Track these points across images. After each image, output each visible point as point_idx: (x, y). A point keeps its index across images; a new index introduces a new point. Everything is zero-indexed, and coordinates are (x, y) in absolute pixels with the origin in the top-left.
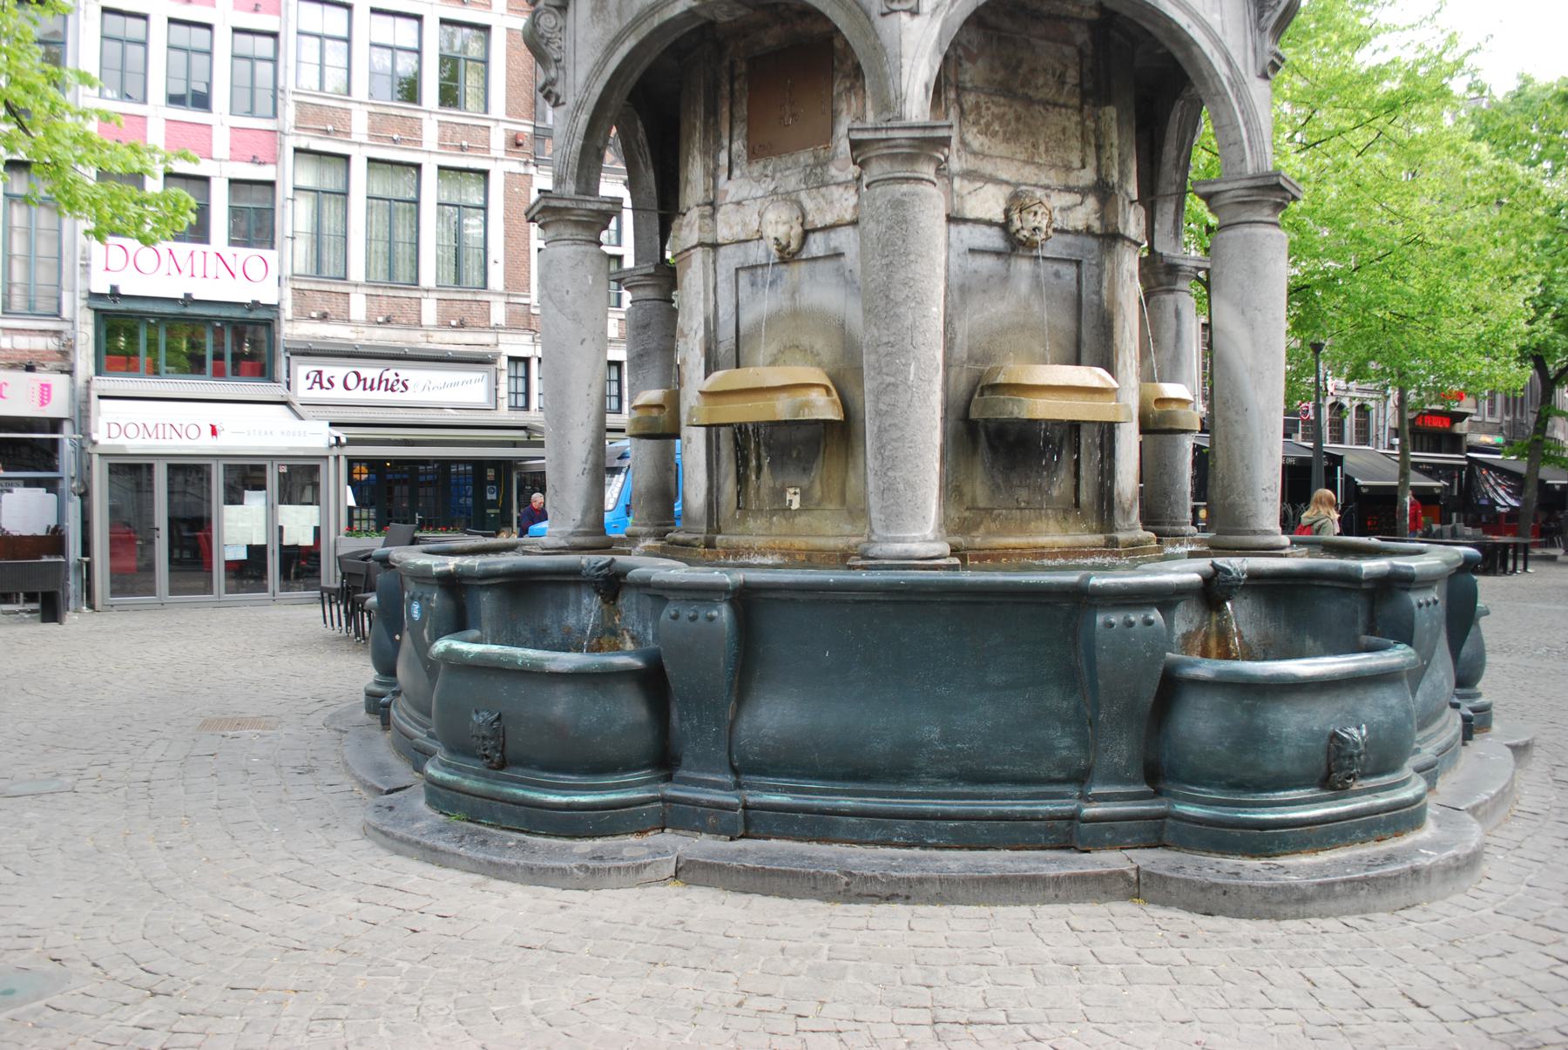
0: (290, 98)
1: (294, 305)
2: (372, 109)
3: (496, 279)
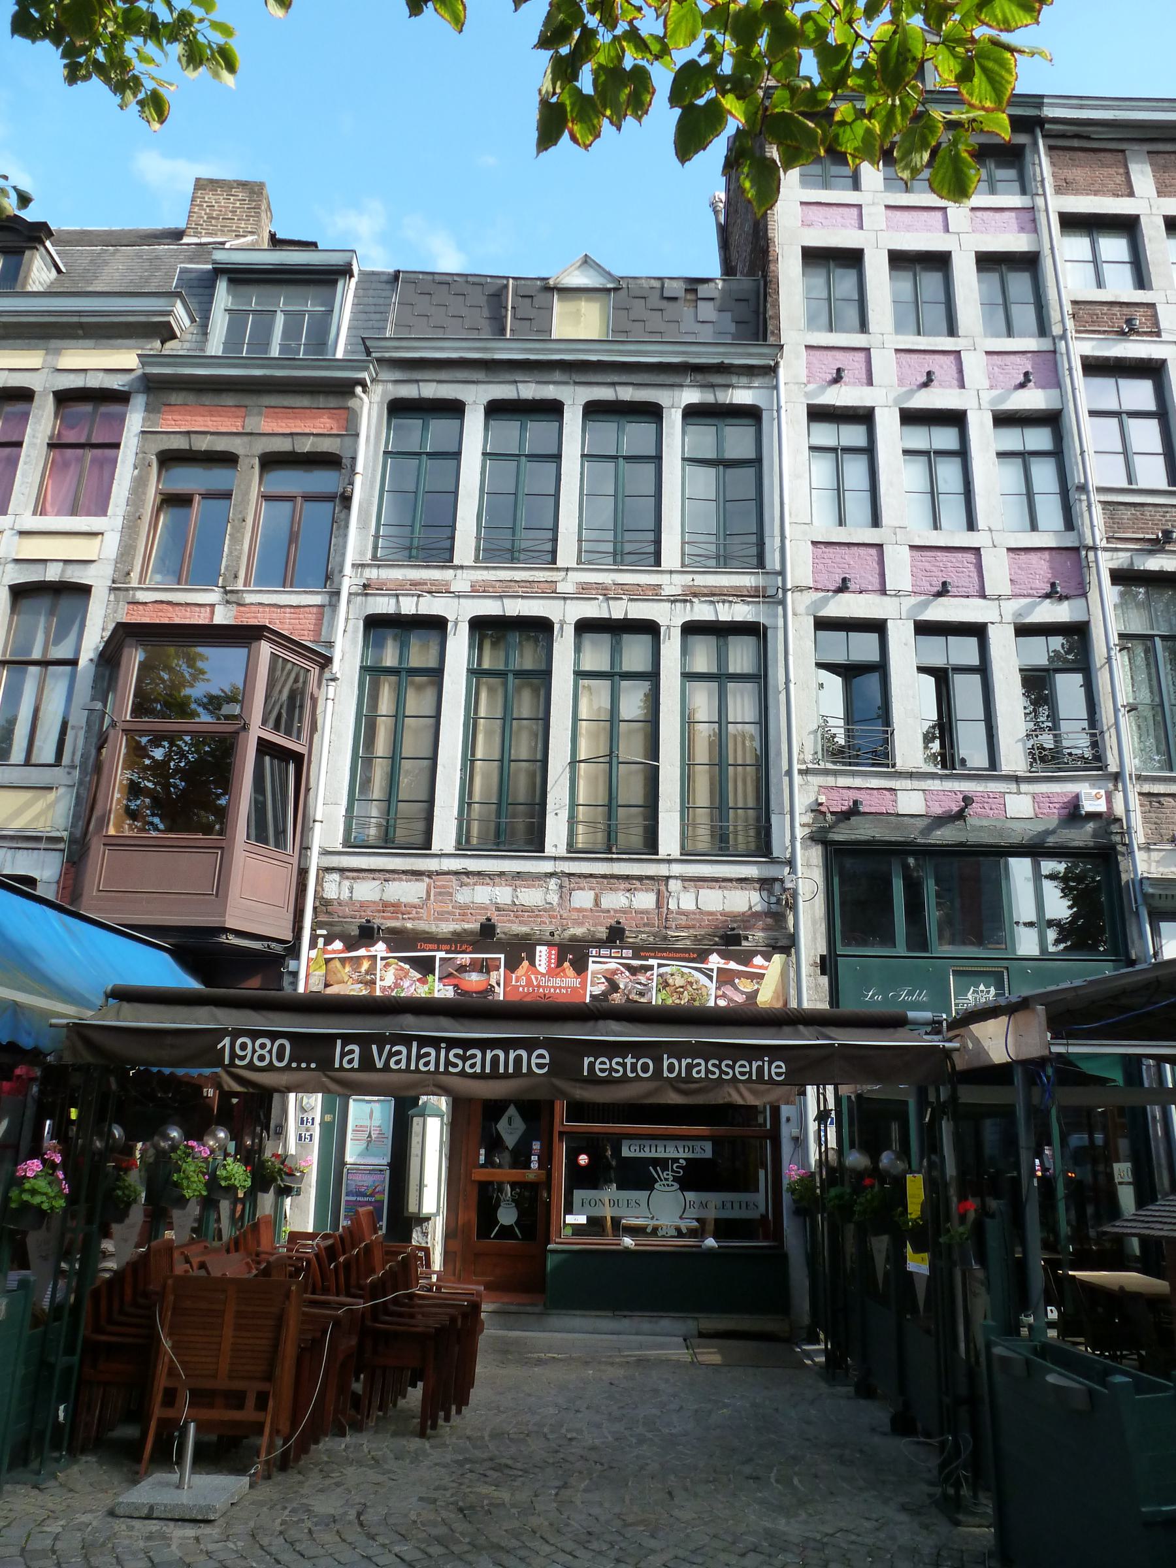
0: (1095, 497)
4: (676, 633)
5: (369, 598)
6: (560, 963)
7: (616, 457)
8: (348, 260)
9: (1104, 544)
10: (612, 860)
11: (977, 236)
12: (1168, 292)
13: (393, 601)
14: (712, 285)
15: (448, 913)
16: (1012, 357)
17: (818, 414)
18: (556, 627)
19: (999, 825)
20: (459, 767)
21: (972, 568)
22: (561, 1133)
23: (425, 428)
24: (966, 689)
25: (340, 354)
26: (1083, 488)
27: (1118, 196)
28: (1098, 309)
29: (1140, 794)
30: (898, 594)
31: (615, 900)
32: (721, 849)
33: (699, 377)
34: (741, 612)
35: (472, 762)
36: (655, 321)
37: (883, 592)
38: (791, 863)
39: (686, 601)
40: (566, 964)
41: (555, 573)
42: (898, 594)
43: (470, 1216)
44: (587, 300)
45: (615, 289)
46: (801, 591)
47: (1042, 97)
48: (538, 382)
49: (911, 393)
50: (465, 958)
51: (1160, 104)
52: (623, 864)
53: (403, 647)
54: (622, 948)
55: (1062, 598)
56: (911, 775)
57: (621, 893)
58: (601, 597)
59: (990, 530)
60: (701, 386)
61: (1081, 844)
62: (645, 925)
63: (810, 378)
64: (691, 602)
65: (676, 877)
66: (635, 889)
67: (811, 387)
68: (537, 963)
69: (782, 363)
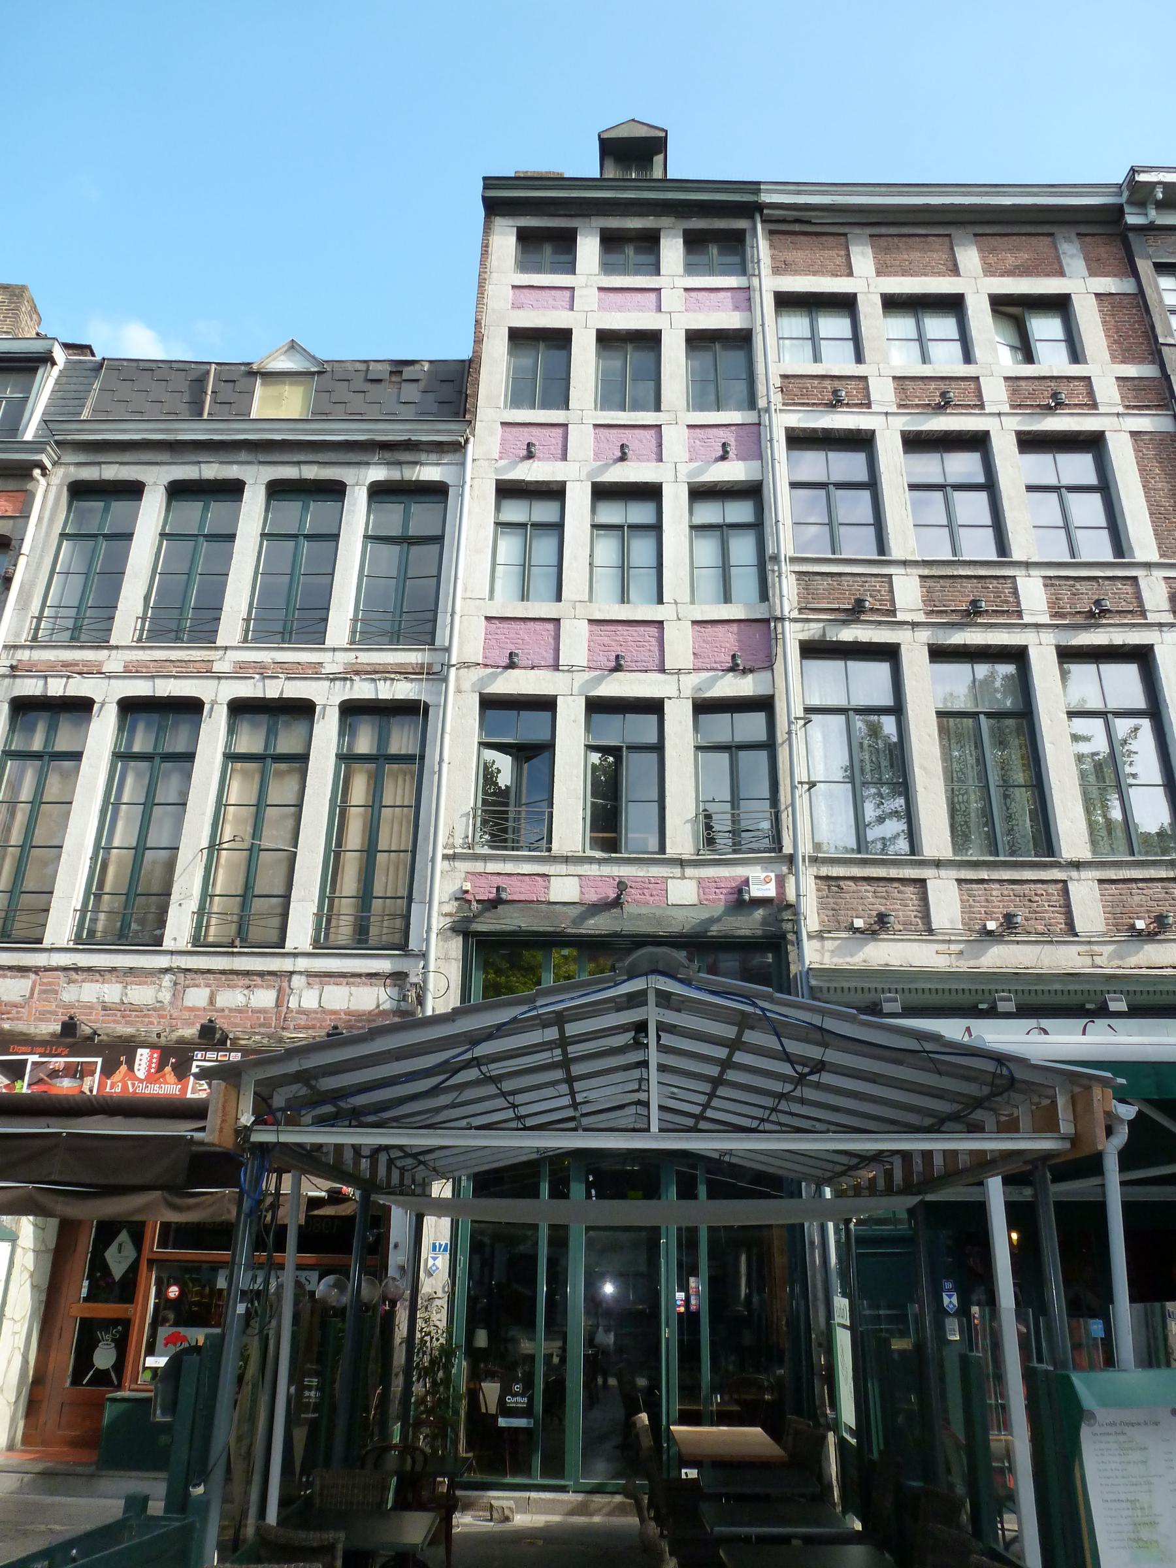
0: (786, 568)
1: (822, 906)
2: (926, 572)
4: (333, 716)
5: (18, 681)
6: (160, 1068)
7: (295, 536)
8: (48, 347)
9: (795, 614)
10: (233, 953)
11: (691, 315)
12: (881, 366)
13: (41, 682)
14: (417, 367)
15: (50, 1012)
16: (715, 430)
17: (507, 491)
18: (207, 708)
19: (658, 912)
20: (90, 854)
21: (654, 642)
22: (151, 1262)
23: (106, 510)
24: (636, 767)
25: (29, 436)
26: (775, 559)
27: (837, 276)
28: (808, 383)
29: (817, 877)
30: (571, 669)
31: (231, 998)
32: (360, 941)
33: (388, 455)
34: (403, 690)
35: (108, 849)
36: (357, 403)
37: (556, 667)
38: (424, 956)
39: (345, 679)
40: (168, 1069)
41: (213, 652)
42: (571, 669)
43: (64, 1359)
44: (292, 384)
45: (319, 373)
46: (468, 667)
47: (759, 183)
48: (221, 463)
49: (607, 466)
50: (59, 1062)
51: (877, 189)
52: (245, 959)
53: (52, 729)
54: (230, 1051)
55: (744, 672)
56: (566, 860)
57: (238, 991)
58: (257, 676)
59: (676, 603)
60: (388, 464)
61: (748, 933)
62: (261, 1025)
63: (503, 454)
64: (351, 680)
65: (300, 973)
66: (255, 986)
67: (503, 462)
68: (136, 1067)
69: (472, 439)
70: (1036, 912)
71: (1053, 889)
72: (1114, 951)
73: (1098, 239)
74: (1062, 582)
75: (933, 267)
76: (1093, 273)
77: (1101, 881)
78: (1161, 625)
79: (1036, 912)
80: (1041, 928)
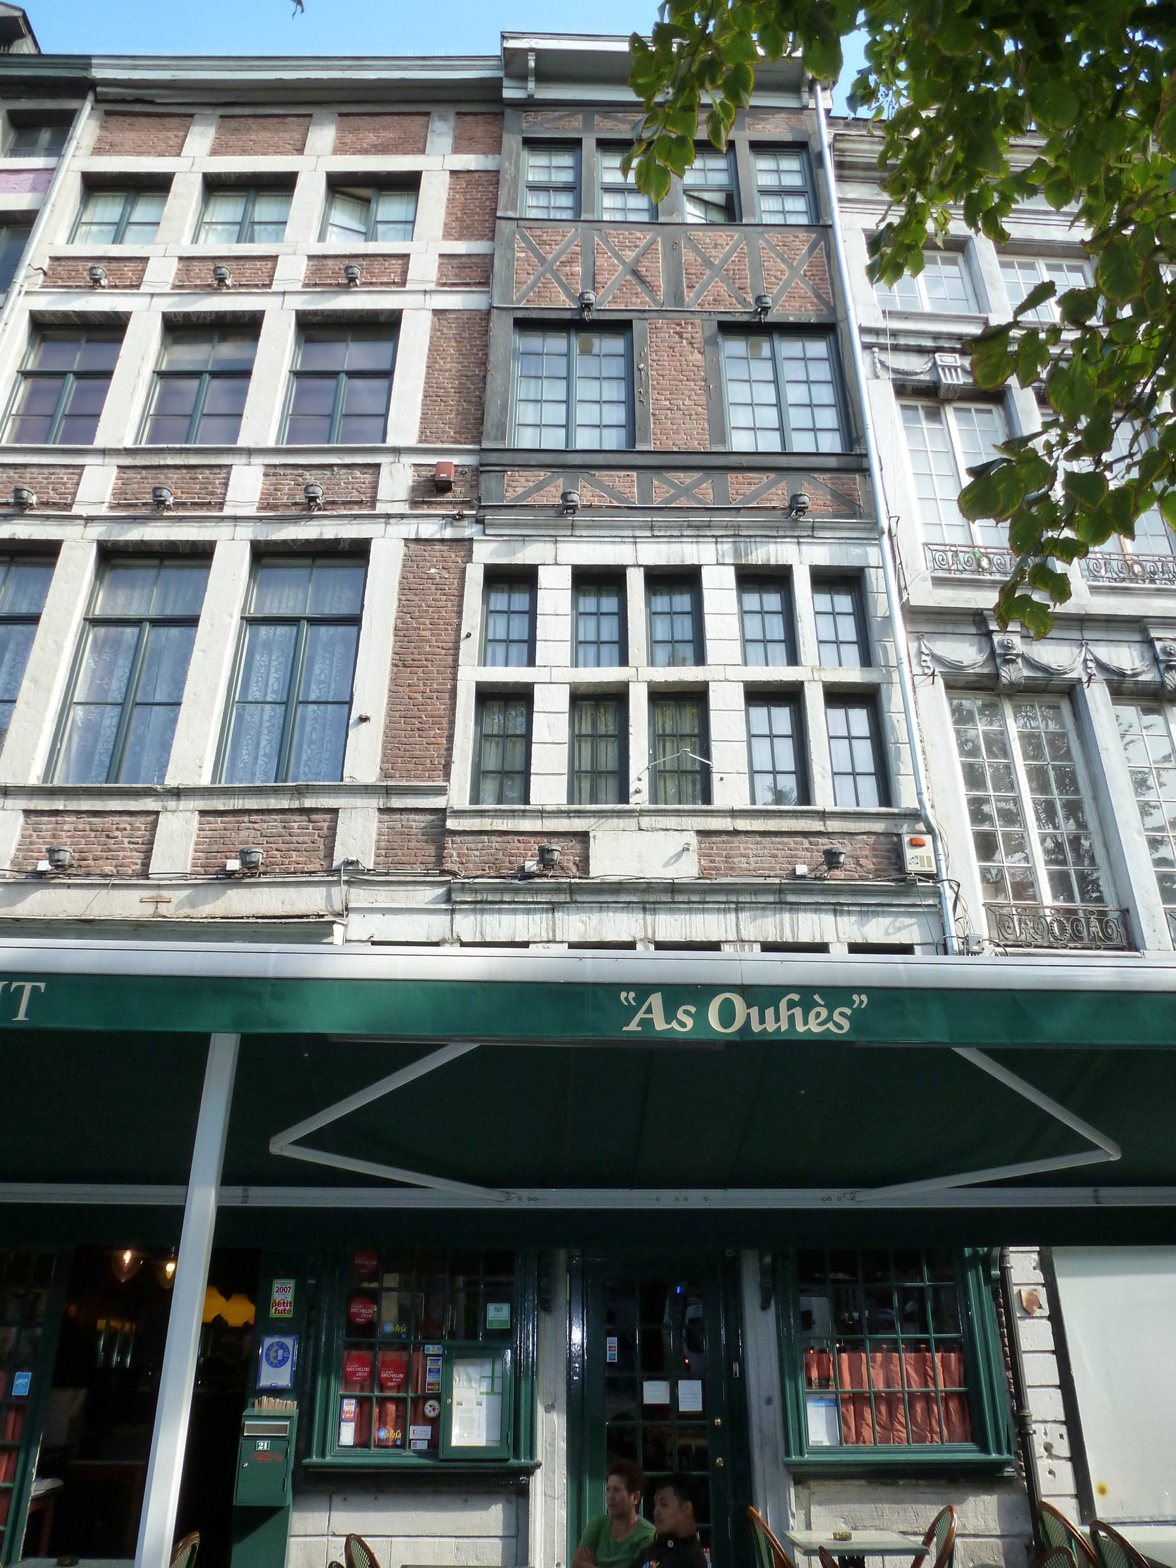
2: (127, 461)
3: (364, 758)
47: (89, 57)
51: (224, 63)
70: (110, 850)
71: (140, 822)
72: (188, 897)
73: (480, 119)
74: (288, 471)
75: (278, 147)
76: (457, 149)
77: (203, 813)
78: (388, 516)
79: (110, 850)
80: (108, 869)
